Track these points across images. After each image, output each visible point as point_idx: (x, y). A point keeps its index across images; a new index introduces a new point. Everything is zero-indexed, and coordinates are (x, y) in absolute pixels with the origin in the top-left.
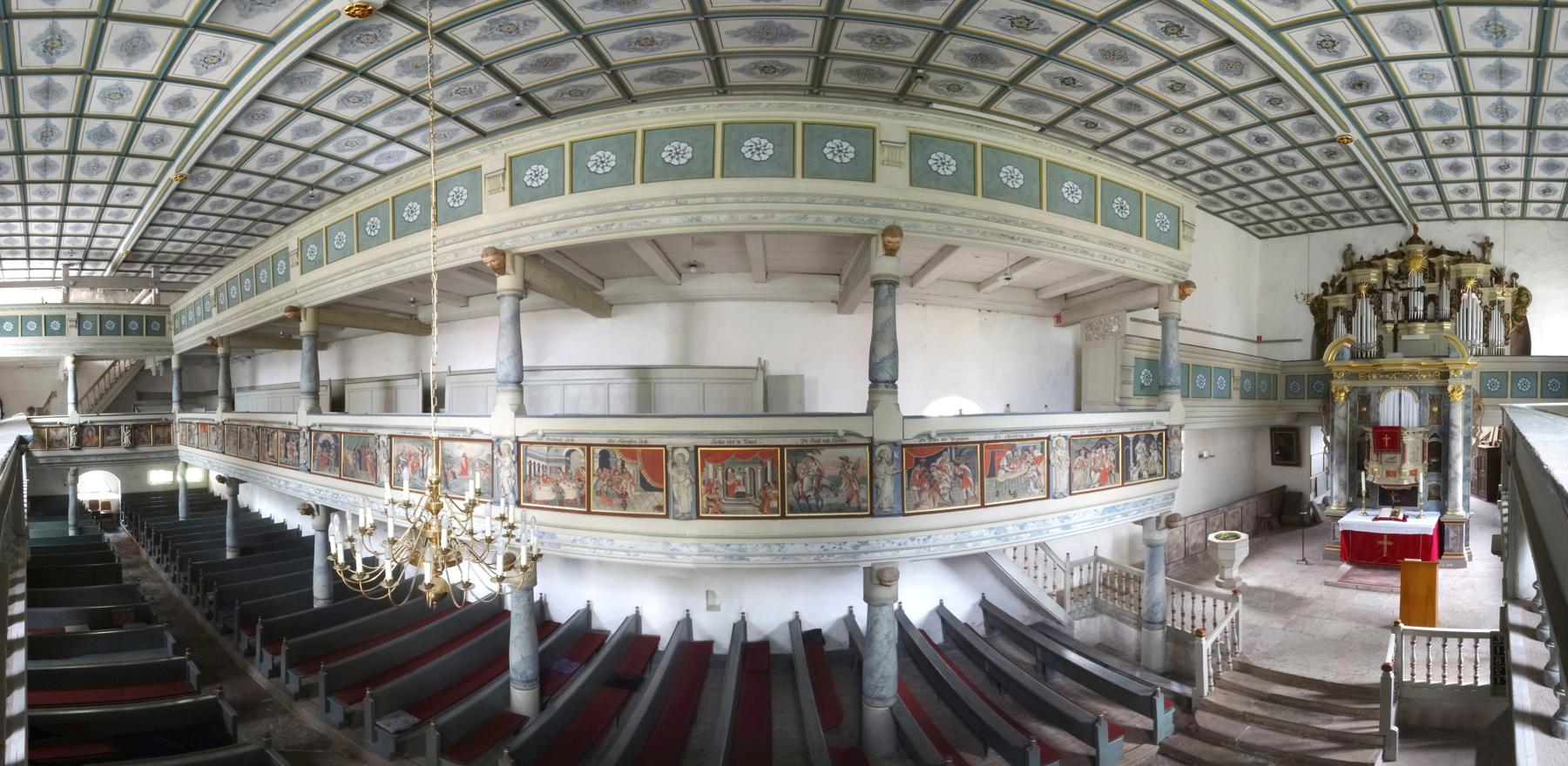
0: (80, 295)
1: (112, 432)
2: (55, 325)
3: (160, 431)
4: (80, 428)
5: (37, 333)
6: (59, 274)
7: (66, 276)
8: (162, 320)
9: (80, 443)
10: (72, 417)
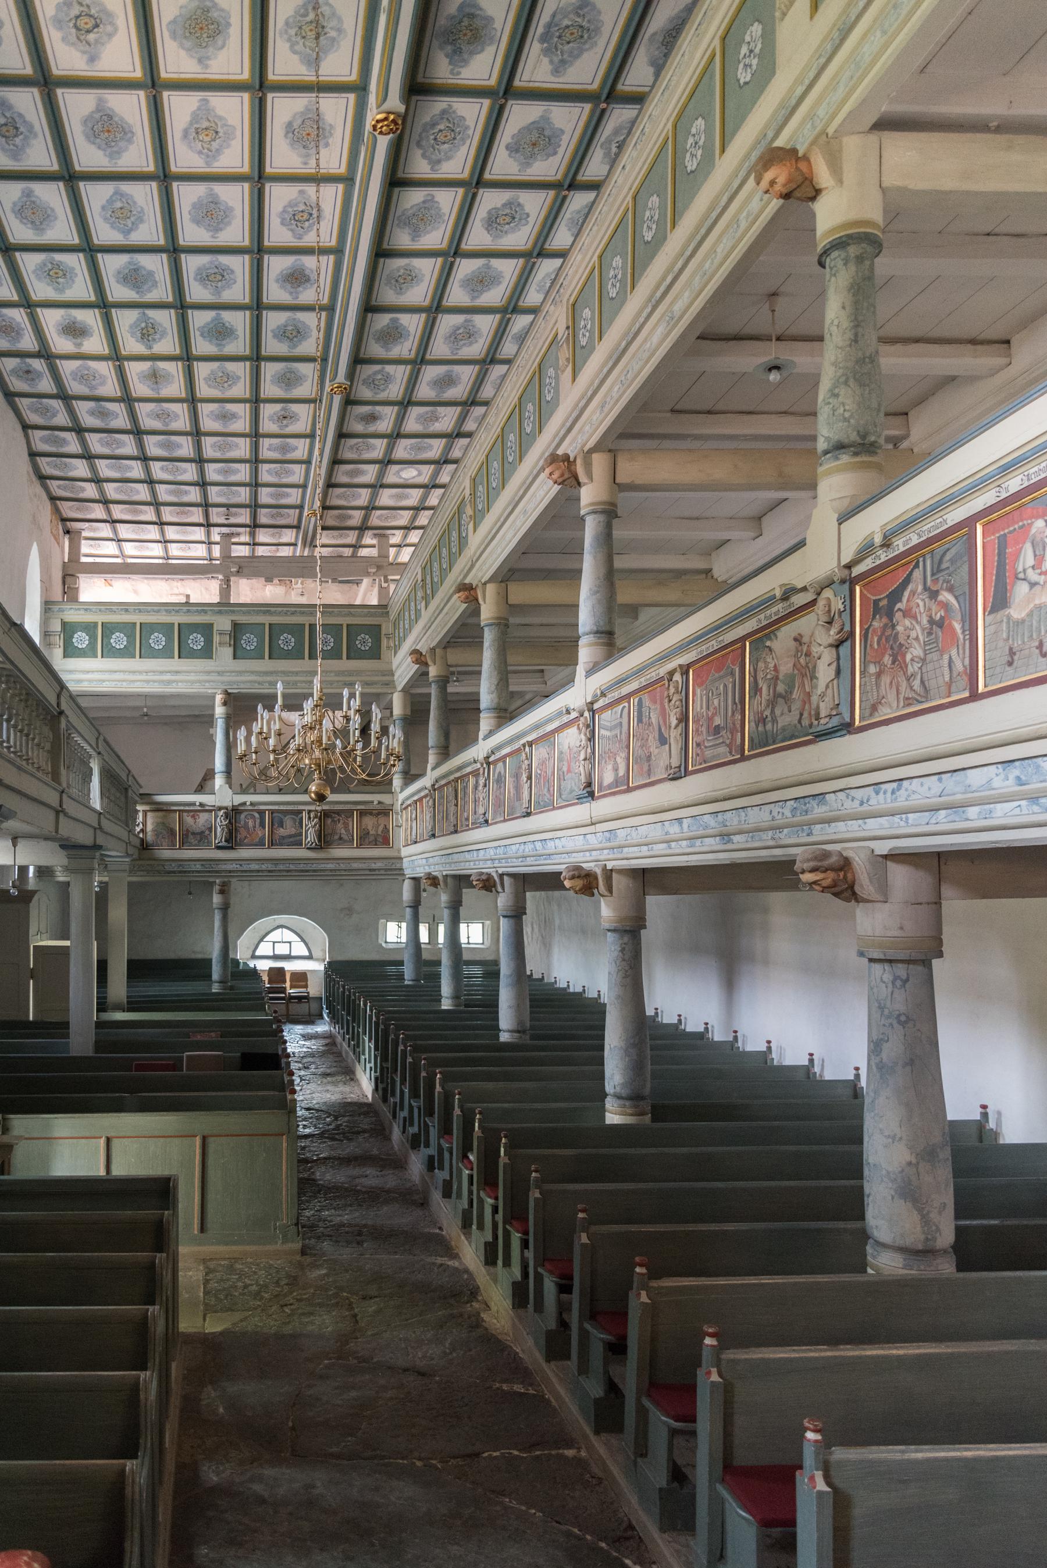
0: (248, 591)
2: (197, 641)
3: (369, 822)
5: (166, 653)
6: (216, 551)
7: (226, 556)
8: (375, 631)
9: (232, 841)
10: (222, 793)
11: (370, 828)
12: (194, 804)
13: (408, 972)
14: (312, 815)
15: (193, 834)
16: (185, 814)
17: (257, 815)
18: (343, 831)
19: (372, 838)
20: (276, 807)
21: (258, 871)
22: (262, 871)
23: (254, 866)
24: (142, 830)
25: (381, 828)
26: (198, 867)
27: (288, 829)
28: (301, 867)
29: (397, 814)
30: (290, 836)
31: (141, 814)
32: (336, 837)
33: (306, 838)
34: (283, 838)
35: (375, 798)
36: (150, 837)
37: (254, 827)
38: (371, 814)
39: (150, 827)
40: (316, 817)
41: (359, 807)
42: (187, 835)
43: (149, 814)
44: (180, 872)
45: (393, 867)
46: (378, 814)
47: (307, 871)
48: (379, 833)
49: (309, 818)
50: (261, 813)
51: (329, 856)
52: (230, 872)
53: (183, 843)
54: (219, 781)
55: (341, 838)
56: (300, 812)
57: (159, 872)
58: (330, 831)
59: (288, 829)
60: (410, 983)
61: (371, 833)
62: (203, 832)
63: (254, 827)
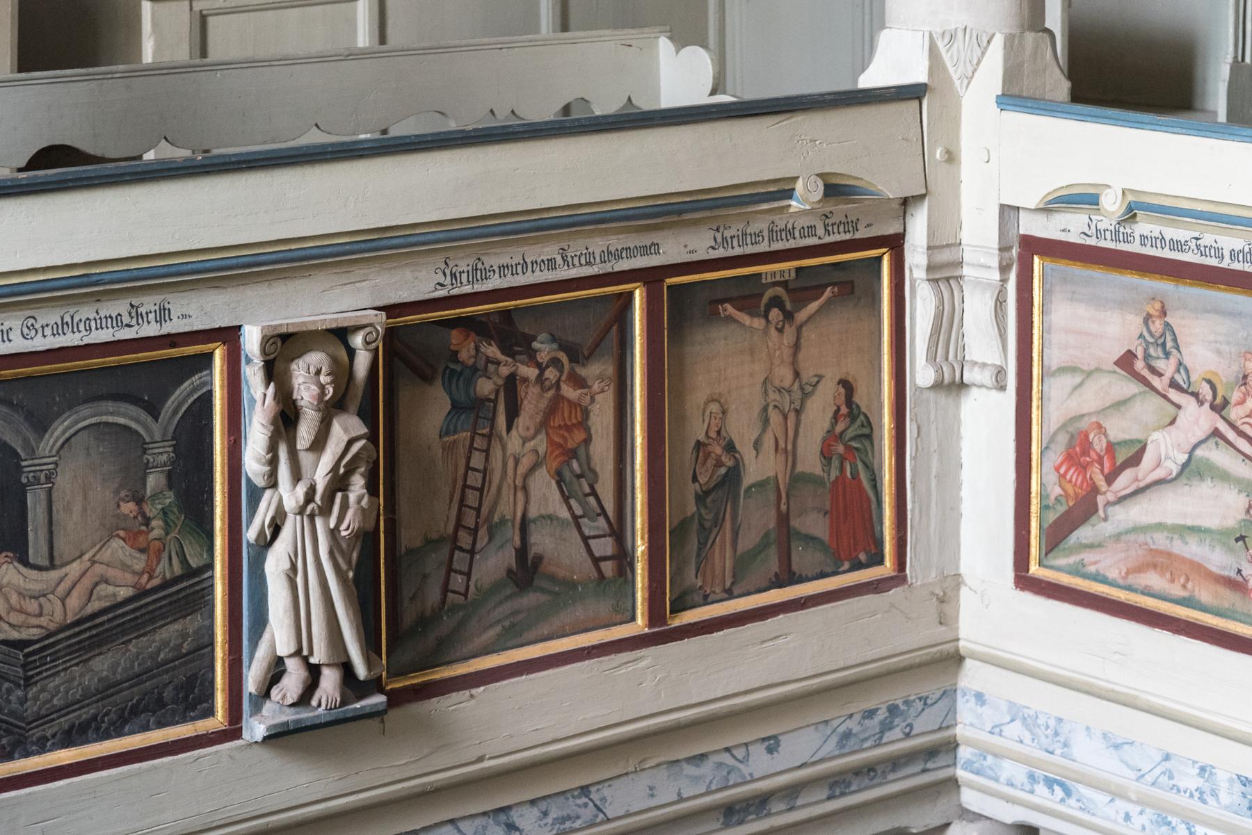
3: (734, 369)
11: (742, 429)
14: (308, 378)
18: (545, 495)
19: (756, 520)
25: (818, 415)
30: (94, 632)
32: (494, 562)
33: (247, 617)
38: (748, 296)
41: (673, 248)
45: (895, 744)
46: (804, 288)
48: (810, 461)
51: (442, 767)
55: (527, 570)
58: (442, 517)
61: (759, 467)
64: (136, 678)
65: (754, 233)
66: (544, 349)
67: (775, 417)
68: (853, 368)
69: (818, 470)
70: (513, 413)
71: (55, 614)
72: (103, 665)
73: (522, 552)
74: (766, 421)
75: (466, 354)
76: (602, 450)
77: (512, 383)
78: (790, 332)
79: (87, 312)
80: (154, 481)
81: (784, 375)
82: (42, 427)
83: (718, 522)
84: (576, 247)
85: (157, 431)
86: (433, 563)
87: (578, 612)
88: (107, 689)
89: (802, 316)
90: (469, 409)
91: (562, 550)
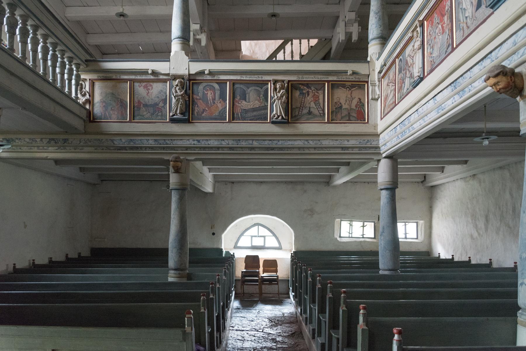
1: (252, 93)
3: (341, 95)
4: (189, 83)
9: (188, 113)
10: (178, 63)
11: (343, 101)
12: (145, 72)
13: (384, 264)
15: (146, 105)
16: (137, 84)
17: (216, 86)
18: (313, 105)
19: (345, 113)
20: (238, 77)
21: (218, 148)
22: (223, 148)
23: (213, 143)
24: (88, 101)
25: (355, 102)
26: (151, 142)
27: (252, 101)
28: (266, 144)
29: (374, 85)
30: (254, 110)
31: (87, 83)
32: (305, 111)
34: (246, 111)
35: (349, 67)
36: (98, 110)
37: (214, 99)
38: (344, 86)
39: (97, 98)
40: (282, 88)
41: (331, 78)
42: (139, 108)
43: (97, 85)
44: (132, 148)
46: (353, 86)
47: (273, 149)
48: (353, 106)
49: (275, 89)
50: (222, 83)
52: (187, 148)
53: (133, 116)
54: (176, 46)
55: (310, 113)
56: (266, 83)
57: (108, 148)
58: (299, 105)
59: (252, 101)
60: (386, 273)
62: (156, 104)
63: (214, 99)
64: (259, 116)
65: (343, 78)
66: (313, 88)
67: (348, 101)
68: (360, 97)
69: (355, 108)
70: (308, 95)
71: (249, 107)
72: (255, 113)
73: (309, 111)
74: (346, 101)
75: (302, 87)
76: (321, 101)
77: (308, 92)
78: (350, 91)
79: (253, 76)
80: (261, 96)
81: (350, 96)
82: (248, 88)
83: (339, 112)
84: (317, 76)
85: (262, 91)
86: (297, 110)
87: (317, 119)
88: (255, 116)
89: (352, 90)
90: (302, 94)
91: (315, 111)
